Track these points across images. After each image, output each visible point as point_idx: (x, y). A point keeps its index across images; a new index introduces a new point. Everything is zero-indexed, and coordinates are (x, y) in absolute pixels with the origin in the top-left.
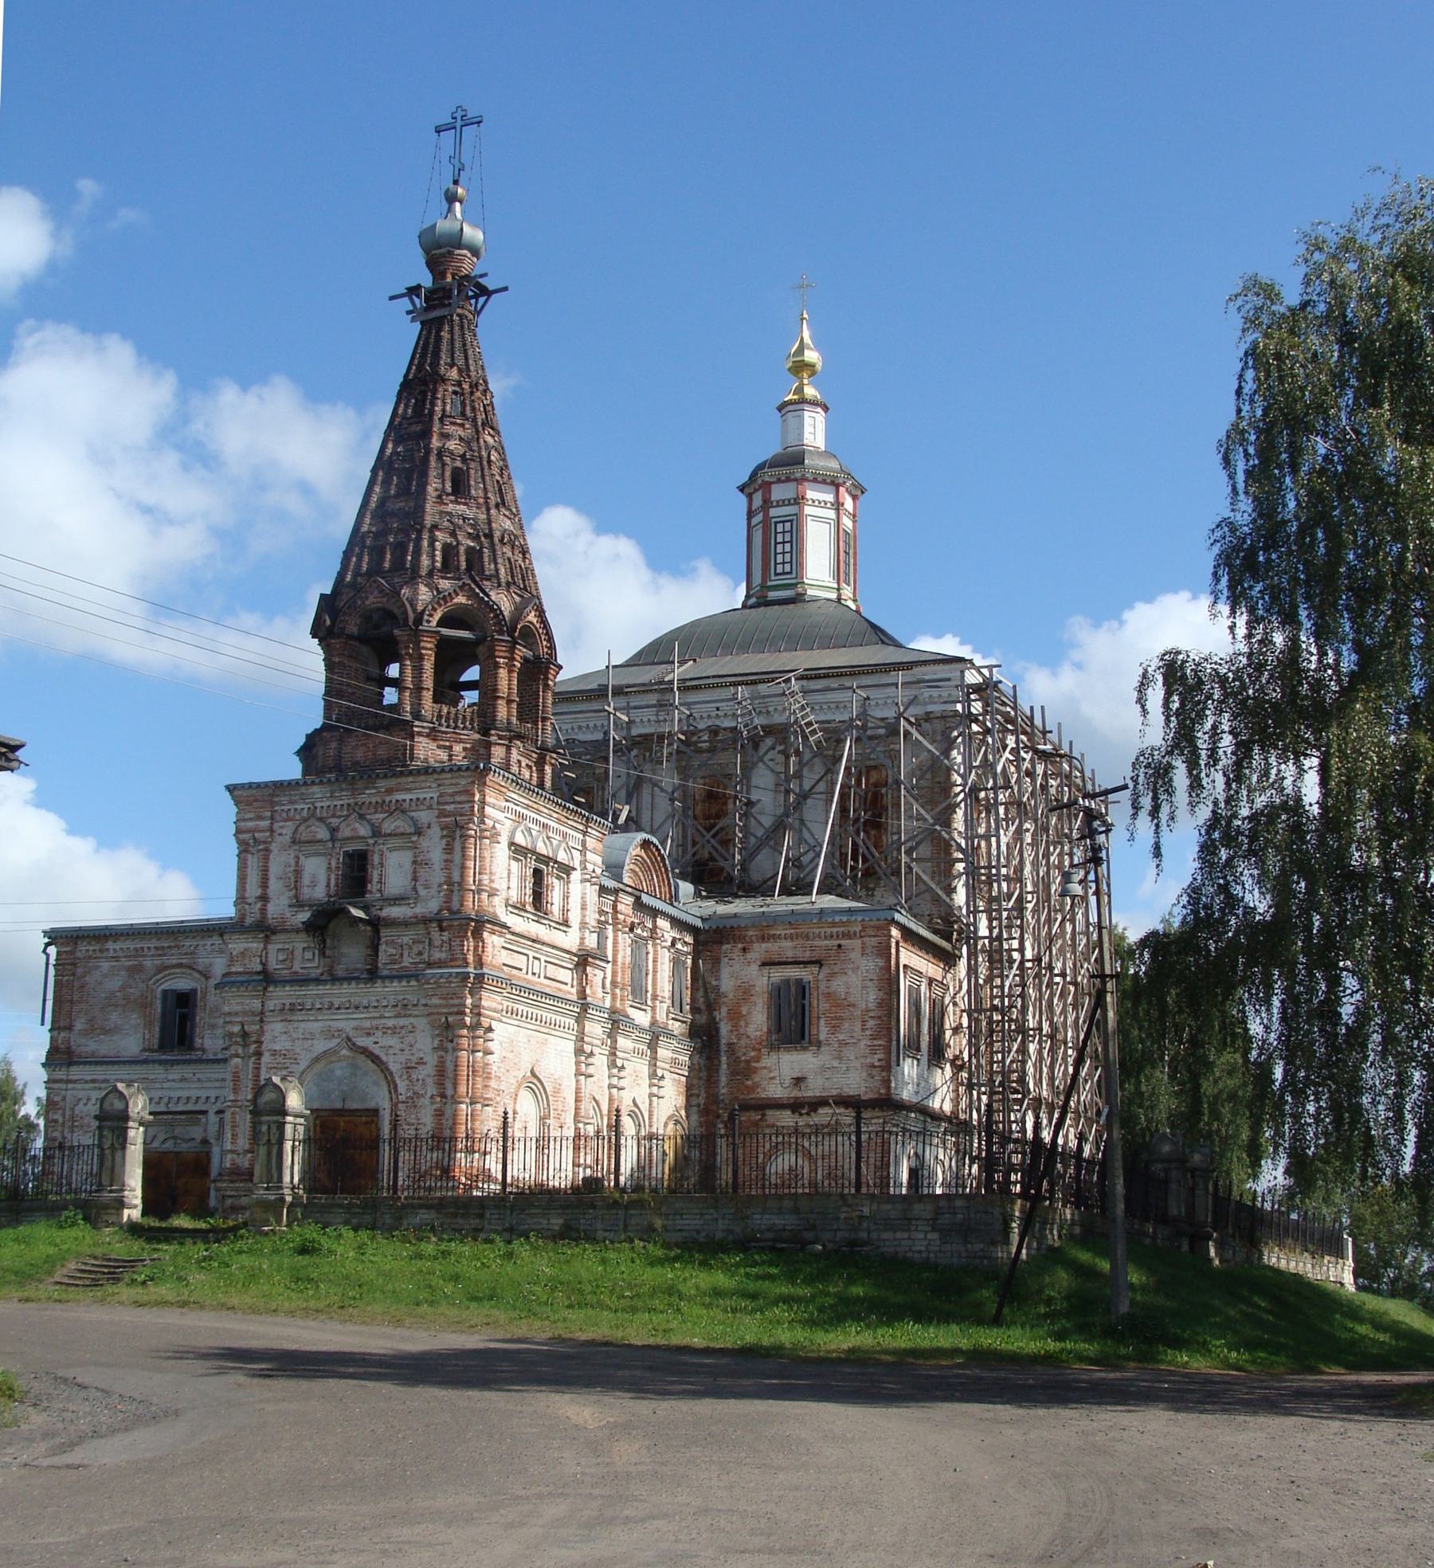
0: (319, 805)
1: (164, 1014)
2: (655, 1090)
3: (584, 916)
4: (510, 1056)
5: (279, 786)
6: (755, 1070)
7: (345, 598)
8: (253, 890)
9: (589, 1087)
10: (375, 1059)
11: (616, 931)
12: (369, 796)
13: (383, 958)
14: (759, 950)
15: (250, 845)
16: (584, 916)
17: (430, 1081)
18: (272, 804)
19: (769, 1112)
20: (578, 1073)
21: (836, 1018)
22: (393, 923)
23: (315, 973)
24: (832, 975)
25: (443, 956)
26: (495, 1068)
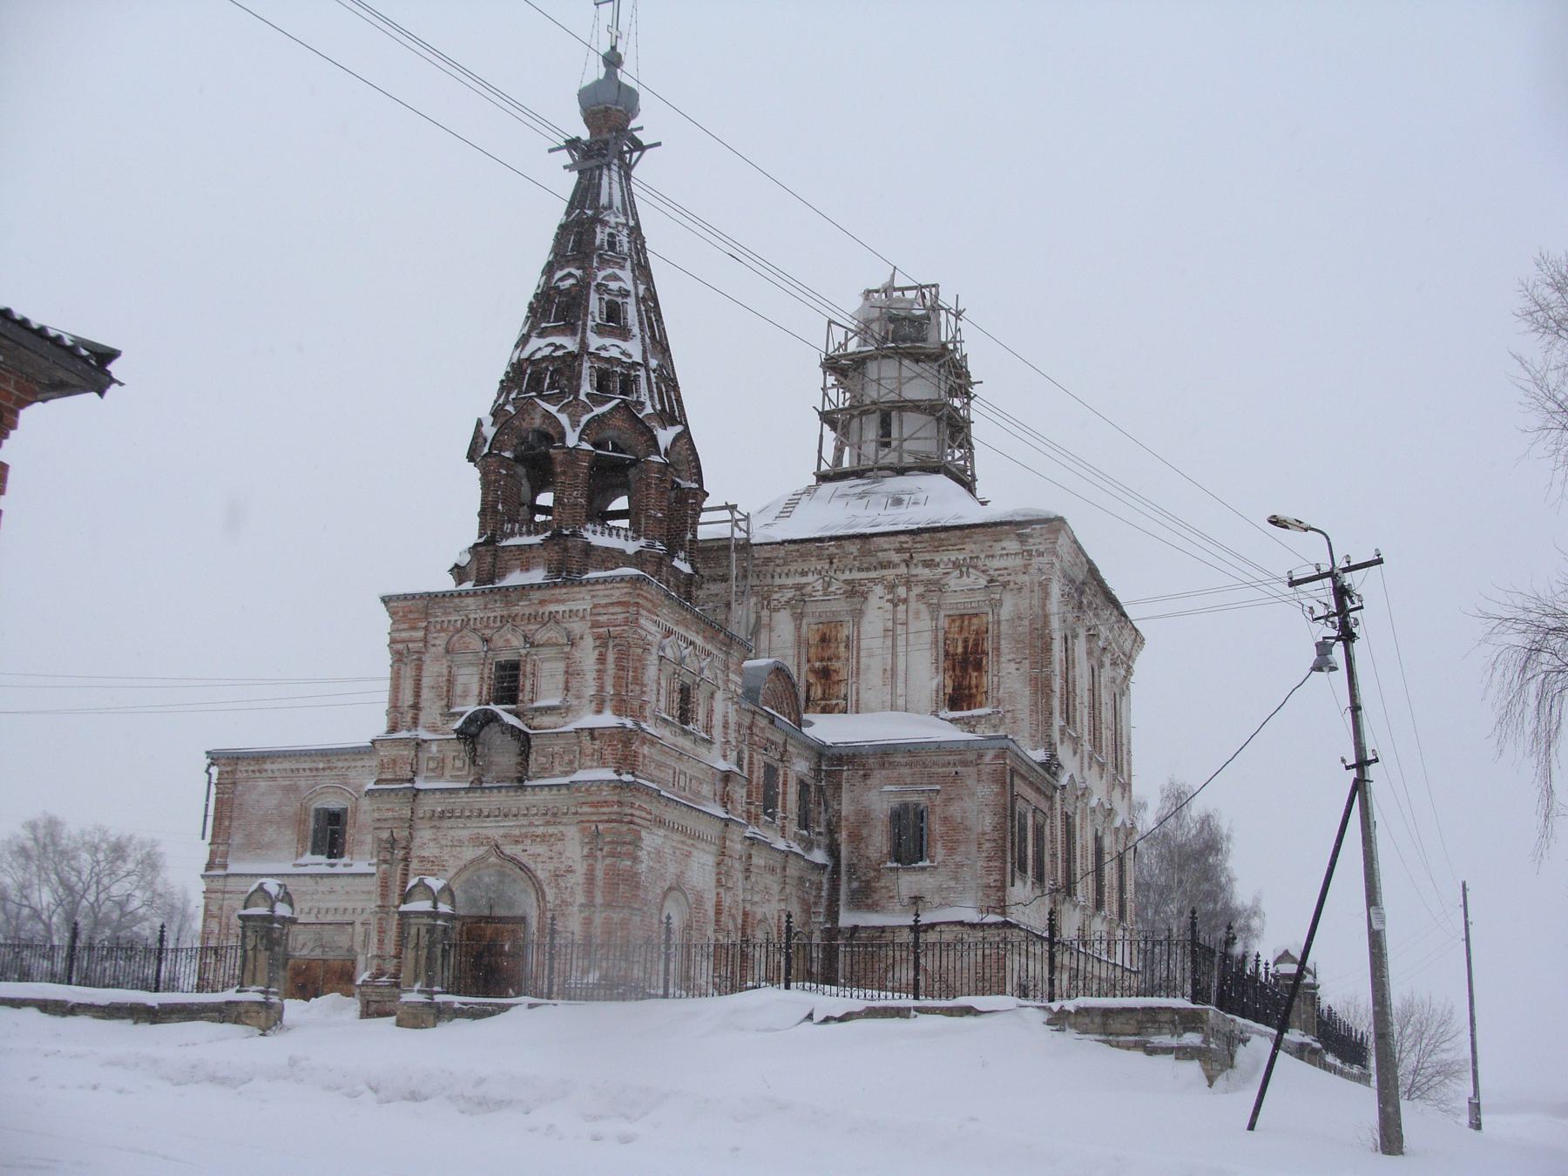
0: (472, 616)
1: (315, 831)
4: (657, 866)
5: (432, 598)
8: (407, 698)
9: (727, 901)
10: (523, 867)
17: (579, 890)
21: (952, 841)
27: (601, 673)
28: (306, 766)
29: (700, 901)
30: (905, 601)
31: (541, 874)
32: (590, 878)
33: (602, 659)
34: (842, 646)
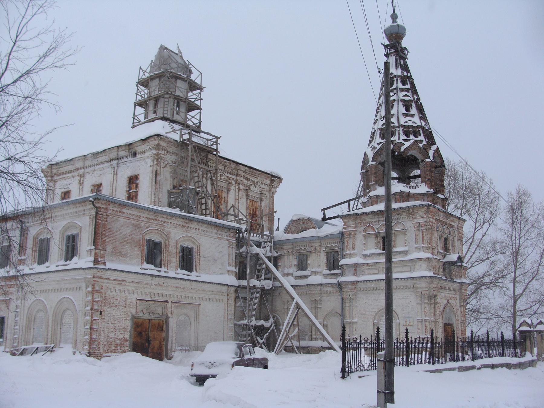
28: (146, 215)
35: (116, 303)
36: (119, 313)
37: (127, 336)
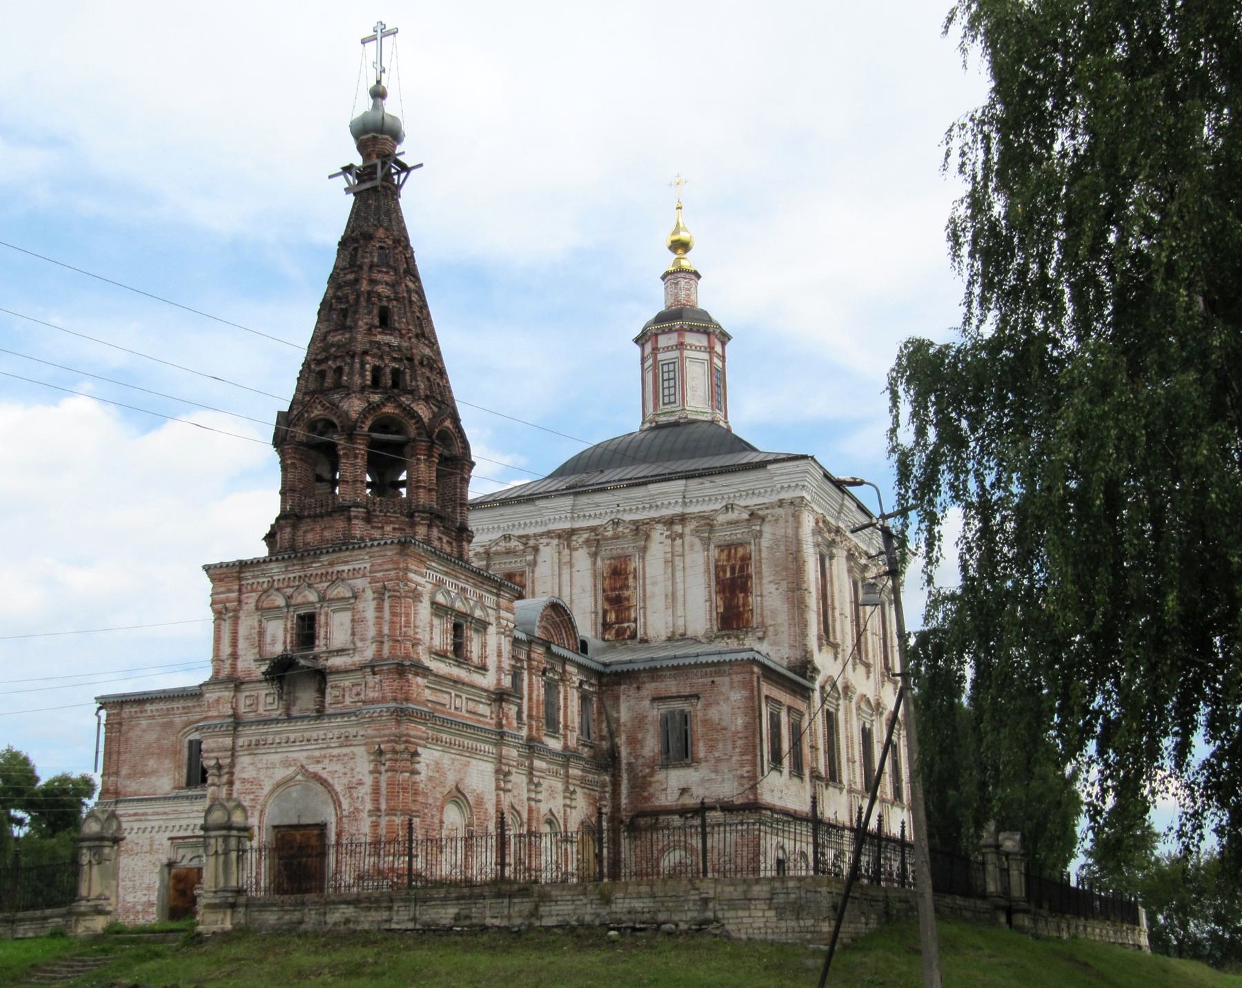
0: (276, 578)
2: (568, 802)
3: (500, 662)
4: (437, 775)
5: (243, 565)
6: (650, 783)
7: (295, 412)
8: (226, 650)
11: (530, 674)
12: (315, 568)
13: (328, 699)
14: (650, 688)
15: (223, 612)
16: (500, 662)
17: (368, 798)
18: (240, 579)
19: (661, 818)
20: (498, 788)
21: (712, 740)
22: (338, 671)
23: (275, 714)
24: (708, 705)
25: (376, 694)
26: (422, 786)
27: (379, 619)
29: (480, 802)
30: (681, 536)
31: (338, 788)
32: (376, 790)
33: (379, 609)
34: (630, 577)
35: (137, 849)
36: (140, 864)
37: (154, 898)
